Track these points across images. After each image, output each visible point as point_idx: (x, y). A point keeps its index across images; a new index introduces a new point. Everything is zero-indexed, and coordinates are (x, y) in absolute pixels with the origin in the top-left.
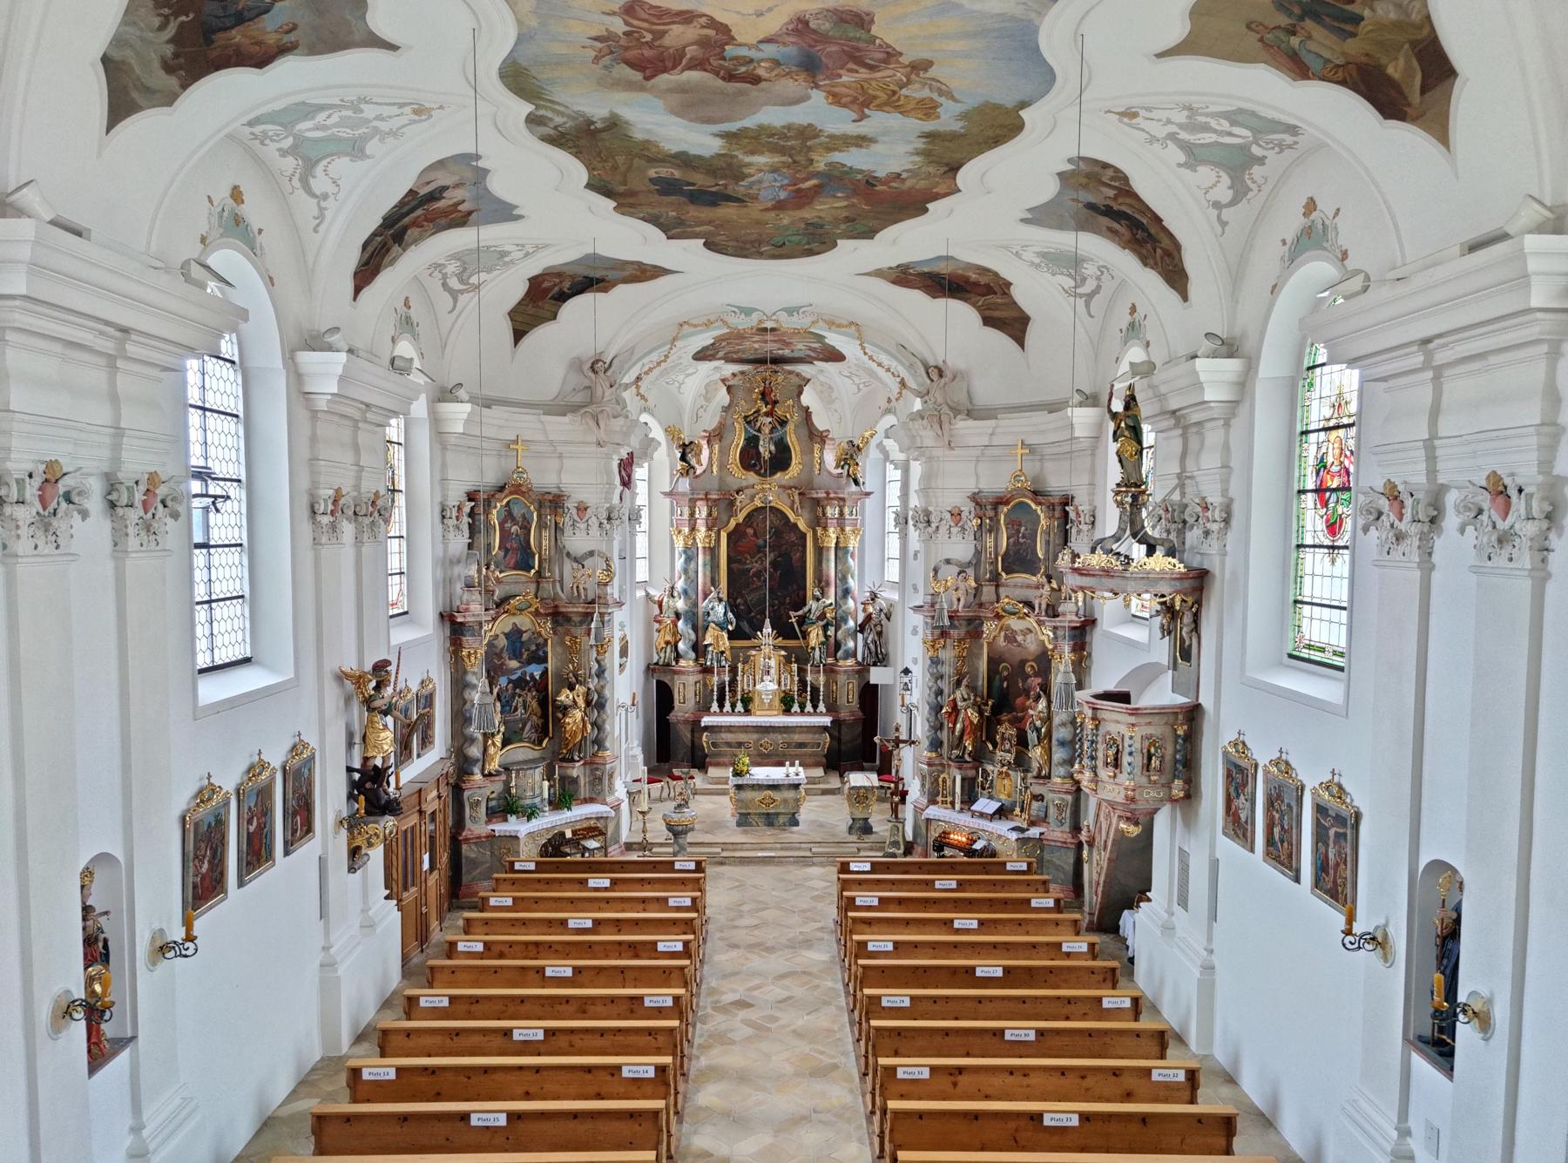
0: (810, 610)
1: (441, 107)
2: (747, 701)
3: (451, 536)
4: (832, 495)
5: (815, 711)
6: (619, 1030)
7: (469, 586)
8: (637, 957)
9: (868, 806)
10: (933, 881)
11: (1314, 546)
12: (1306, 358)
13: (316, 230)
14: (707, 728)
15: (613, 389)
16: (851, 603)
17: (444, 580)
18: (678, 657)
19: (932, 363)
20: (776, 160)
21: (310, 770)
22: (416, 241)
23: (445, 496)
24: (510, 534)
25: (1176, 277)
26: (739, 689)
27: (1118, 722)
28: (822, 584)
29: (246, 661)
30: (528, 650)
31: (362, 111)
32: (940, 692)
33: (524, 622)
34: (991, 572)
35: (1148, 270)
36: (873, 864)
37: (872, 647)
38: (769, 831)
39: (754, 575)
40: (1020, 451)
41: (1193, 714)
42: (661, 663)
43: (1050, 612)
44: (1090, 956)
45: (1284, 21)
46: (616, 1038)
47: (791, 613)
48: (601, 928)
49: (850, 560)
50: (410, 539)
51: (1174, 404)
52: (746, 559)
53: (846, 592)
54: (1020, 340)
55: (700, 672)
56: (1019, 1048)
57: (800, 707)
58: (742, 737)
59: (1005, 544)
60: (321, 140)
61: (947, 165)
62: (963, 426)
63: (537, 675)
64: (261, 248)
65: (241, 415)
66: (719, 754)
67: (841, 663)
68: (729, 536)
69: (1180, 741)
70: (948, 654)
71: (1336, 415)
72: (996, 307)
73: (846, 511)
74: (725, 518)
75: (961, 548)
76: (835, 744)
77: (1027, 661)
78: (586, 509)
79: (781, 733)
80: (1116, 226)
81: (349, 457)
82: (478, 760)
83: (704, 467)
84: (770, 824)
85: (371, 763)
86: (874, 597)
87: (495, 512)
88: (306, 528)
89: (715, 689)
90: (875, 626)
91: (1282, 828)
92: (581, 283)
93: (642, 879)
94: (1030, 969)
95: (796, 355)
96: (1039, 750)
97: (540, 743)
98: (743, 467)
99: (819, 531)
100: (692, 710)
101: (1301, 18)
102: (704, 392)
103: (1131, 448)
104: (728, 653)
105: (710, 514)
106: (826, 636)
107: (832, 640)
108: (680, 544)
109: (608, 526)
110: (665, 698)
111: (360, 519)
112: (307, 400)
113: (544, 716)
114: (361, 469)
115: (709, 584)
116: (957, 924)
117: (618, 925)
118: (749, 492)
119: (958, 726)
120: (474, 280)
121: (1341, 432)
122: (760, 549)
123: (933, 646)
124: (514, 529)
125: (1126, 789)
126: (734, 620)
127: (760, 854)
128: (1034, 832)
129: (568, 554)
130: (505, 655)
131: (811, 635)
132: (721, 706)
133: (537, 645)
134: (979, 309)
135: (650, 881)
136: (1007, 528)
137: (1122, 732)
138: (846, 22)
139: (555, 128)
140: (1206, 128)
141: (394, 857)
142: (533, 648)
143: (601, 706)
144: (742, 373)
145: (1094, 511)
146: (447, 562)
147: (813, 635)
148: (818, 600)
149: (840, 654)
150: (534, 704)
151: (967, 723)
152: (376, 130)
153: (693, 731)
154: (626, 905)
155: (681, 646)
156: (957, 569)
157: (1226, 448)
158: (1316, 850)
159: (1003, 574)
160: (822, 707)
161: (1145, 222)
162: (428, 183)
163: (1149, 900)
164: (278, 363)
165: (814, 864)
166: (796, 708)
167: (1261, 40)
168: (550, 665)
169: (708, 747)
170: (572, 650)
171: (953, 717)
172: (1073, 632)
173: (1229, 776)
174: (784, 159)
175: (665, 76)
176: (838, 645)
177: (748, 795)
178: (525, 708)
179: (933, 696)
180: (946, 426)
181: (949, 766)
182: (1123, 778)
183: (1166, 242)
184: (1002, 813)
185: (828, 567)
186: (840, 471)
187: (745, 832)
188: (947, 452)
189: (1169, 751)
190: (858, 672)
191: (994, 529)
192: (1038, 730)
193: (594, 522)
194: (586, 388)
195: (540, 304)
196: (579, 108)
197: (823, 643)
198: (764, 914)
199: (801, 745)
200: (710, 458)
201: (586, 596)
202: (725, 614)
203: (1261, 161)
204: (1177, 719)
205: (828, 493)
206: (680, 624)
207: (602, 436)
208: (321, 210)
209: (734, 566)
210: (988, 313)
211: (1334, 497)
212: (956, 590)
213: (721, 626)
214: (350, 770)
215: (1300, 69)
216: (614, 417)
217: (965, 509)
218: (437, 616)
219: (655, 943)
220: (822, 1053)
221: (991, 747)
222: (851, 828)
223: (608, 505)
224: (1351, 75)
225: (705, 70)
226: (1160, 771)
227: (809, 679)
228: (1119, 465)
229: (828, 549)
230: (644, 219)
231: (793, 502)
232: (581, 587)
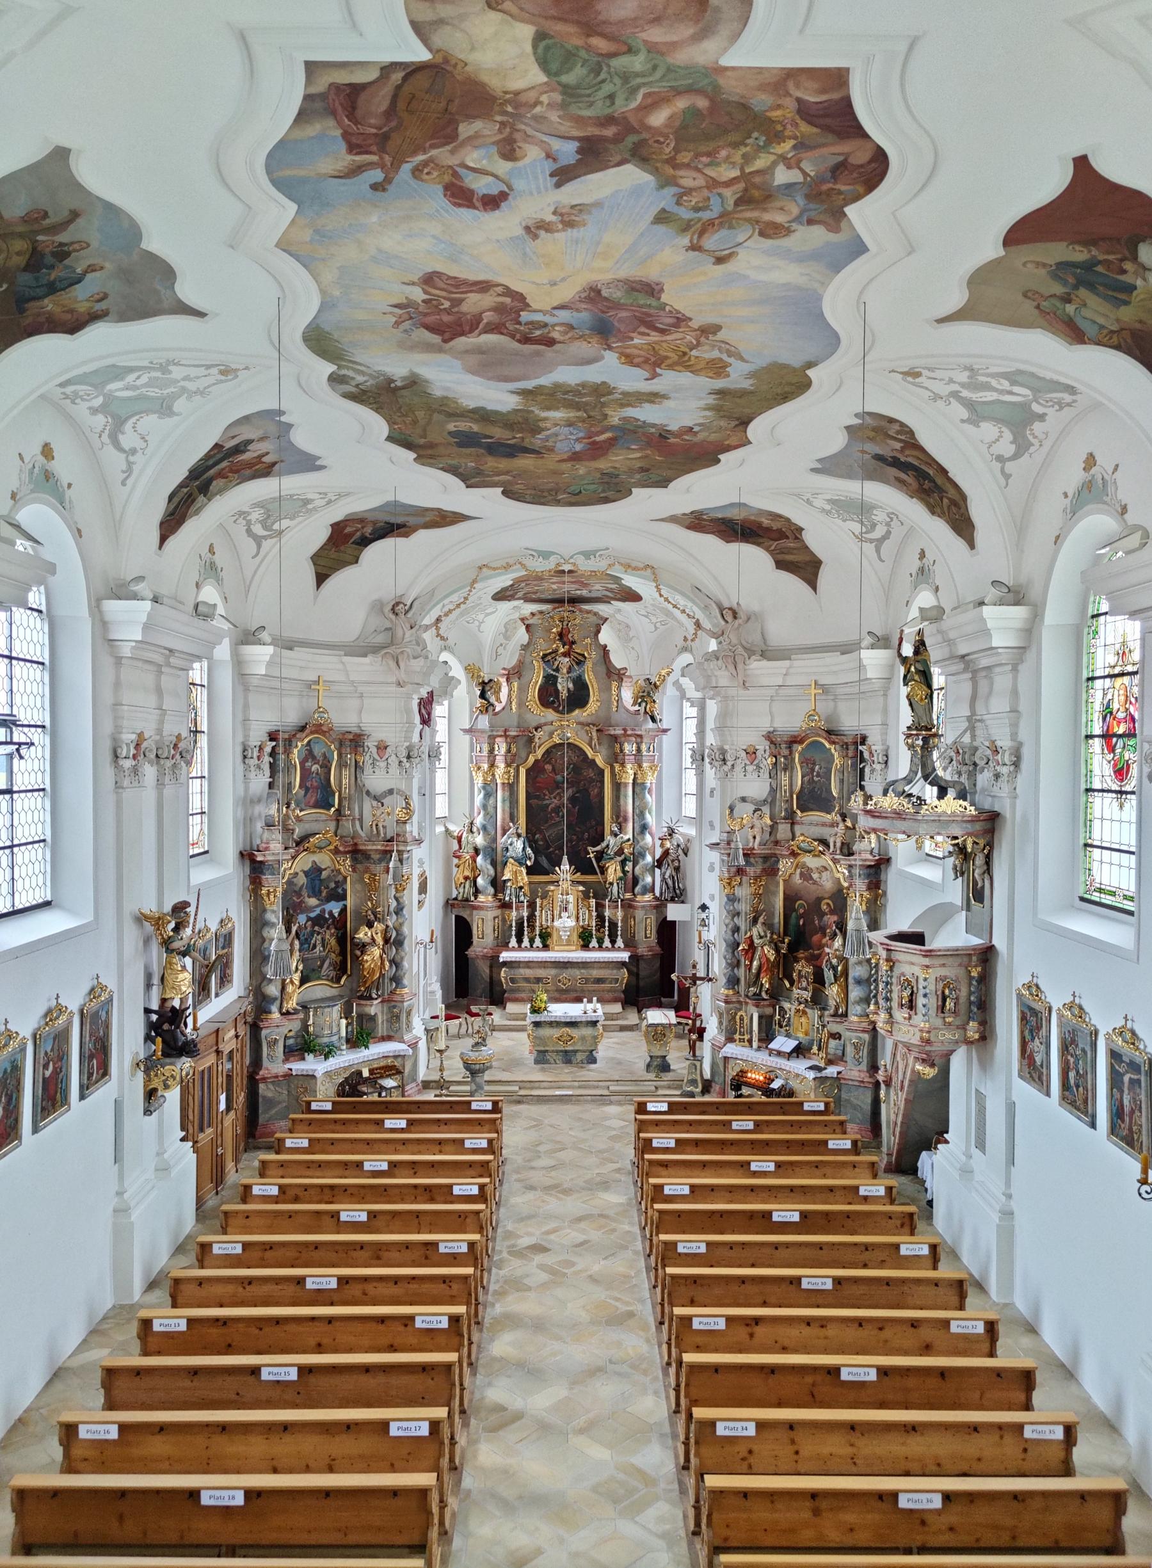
0: (608, 846)
1: (247, 368)
2: (545, 936)
3: (252, 775)
4: (629, 732)
6: (414, 1278)
7: (269, 825)
8: (432, 1200)
9: (666, 1044)
10: (730, 1122)
11: (1103, 791)
12: (1091, 606)
13: (124, 483)
14: (505, 964)
15: (414, 630)
16: (648, 838)
17: (245, 819)
18: (477, 892)
19: (726, 604)
20: (572, 415)
21: (107, 1013)
22: (220, 492)
23: (246, 736)
24: (311, 773)
25: (963, 526)
26: (538, 924)
27: (913, 964)
28: (620, 819)
29: (47, 904)
30: (327, 887)
31: (170, 372)
32: (736, 929)
33: (324, 860)
34: (786, 810)
35: (936, 518)
36: (670, 1104)
37: (670, 882)
38: (567, 1069)
39: (553, 810)
40: (813, 692)
41: (987, 955)
42: (460, 898)
43: (845, 851)
44: (887, 1200)
45: (1059, 289)
46: (411, 1286)
48: (396, 1171)
49: (648, 796)
50: (211, 779)
51: (962, 650)
53: (644, 828)
54: (812, 582)
55: (499, 907)
56: (816, 1298)
58: (541, 973)
59: (800, 782)
60: (129, 399)
61: (738, 419)
62: (757, 666)
63: (336, 912)
64: (70, 502)
65: (47, 662)
66: (518, 990)
67: (639, 898)
68: (528, 772)
69: (974, 983)
70: (744, 892)
71: (1120, 663)
72: (789, 551)
73: (644, 747)
74: (523, 754)
75: (756, 786)
76: (634, 979)
77: (822, 898)
78: (386, 748)
79: (579, 968)
80: (903, 476)
81: (152, 701)
82: (275, 999)
83: (504, 703)
84: (568, 1061)
85: (168, 1005)
86: (671, 832)
87: (295, 751)
88: (109, 772)
90: (673, 861)
91: (1078, 1072)
92: (382, 528)
93: (439, 1120)
94: (827, 1214)
95: (593, 595)
96: (835, 988)
97: (338, 981)
98: (543, 705)
99: (617, 767)
100: (490, 945)
101: (1076, 287)
102: (504, 630)
103: (921, 692)
104: (526, 888)
105: (509, 751)
106: (624, 872)
107: (630, 875)
108: (479, 781)
109: (408, 765)
110: (463, 932)
111: (162, 762)
112: (112, 646)
113: (343, 953)
114: (163, 712)
115: (508, 819)
116: (754, 1167)
117: (414, 1168)
118: (545, 728)
119: (755, 963)
120: (276, 526)
121: (1126, 680)
122: (558, 785)
123: (729, 884)
124: (315, 768)
125: (921, 1031)
126: (533, 856)
127: (557, 1093)
128: (832, 1071)
129: (368, 793)
130: (305, 893)
131: (609, 870)
132: (520, 941)
133: (337, 883)
134: (772, 553)
135: (446, 1122)
136: (802, 767)
137: (916, 974)
138: (637, 291)
139: (357, 386)
140: (987, 387)
141: (191, 1098)
142: (332, 885)
143: (399, 943)
144: (541, 612)
145: (887, 750)
146: (248, 802)
147: (611, 871)
148: (616, 835)
149: (637, 889)
150: (333, 941)
151: (763, 960)
152: (184, 390)
153: (491, 967)
154: (422, 1147)
155: (480, 881)
156: (753, 807)
157: (1015, 693)
158: (1111, 1096)
159: (798, 812)
160: (620, 943)
161: (931, 473)
162: (233, 437)
163: (947, 1142)
164: (84, 612)
165: (611, 1103)
166: (594, 943)
167: (1038, 307)
168: (349, 902)
169: (507, 983)
170: (372, 887)
171: (750, 955)
172: (868, 871)
173: (1023, 1019)
174: (579, 414)
175: (463, 339)
176: (635, 881)
177: (546, 1032)
178: (323, 946)
179: (730, 933)
180: (740, 666)
181: (747, 1003)
182: (918, 1020)
183: (952, 492)
184: (799, 1051)
185: (626, 803)
186: (637, 708)
187: (543, 1070)
188: (742, 692)
189: (964, 992)
190: (656, 907)
191: (788, 767)
192: (834, 968)
193: (393, 760)
194: (387, 629)
195: (342, 548)
196: (380, 368)
197: (620, 879)
198: (562, 1155)
199: (599, 981)
200: (510, 696)
201: (385, 834)
202: (524, 849)
203: (1042, 417)
204: (970, 960)
205: (625, 730)
206: (479, 859)
207: (402, 676)
208: (130, 464)
209: (533, 802)
210: (780, 557)
211: (1120, 743)
212: (752, 828)
213: (520, 862)
214: (148, 1011)
215: (1076, 334)
216: (415, 658)
217: (760, 748)
218: (237, 853)
219: (450, 1187)
220: (617, 1299)
221: (788, 985)
222: (648, 1066)
223: (407, 744)
224: (1125, 341)
225: (502, 334)
226: (955, 1012)
227: (607, 913)
228: (909, 708)
229: (626, 784)
230: (442, 469)
231: (591, 738)
232: (380, 825)
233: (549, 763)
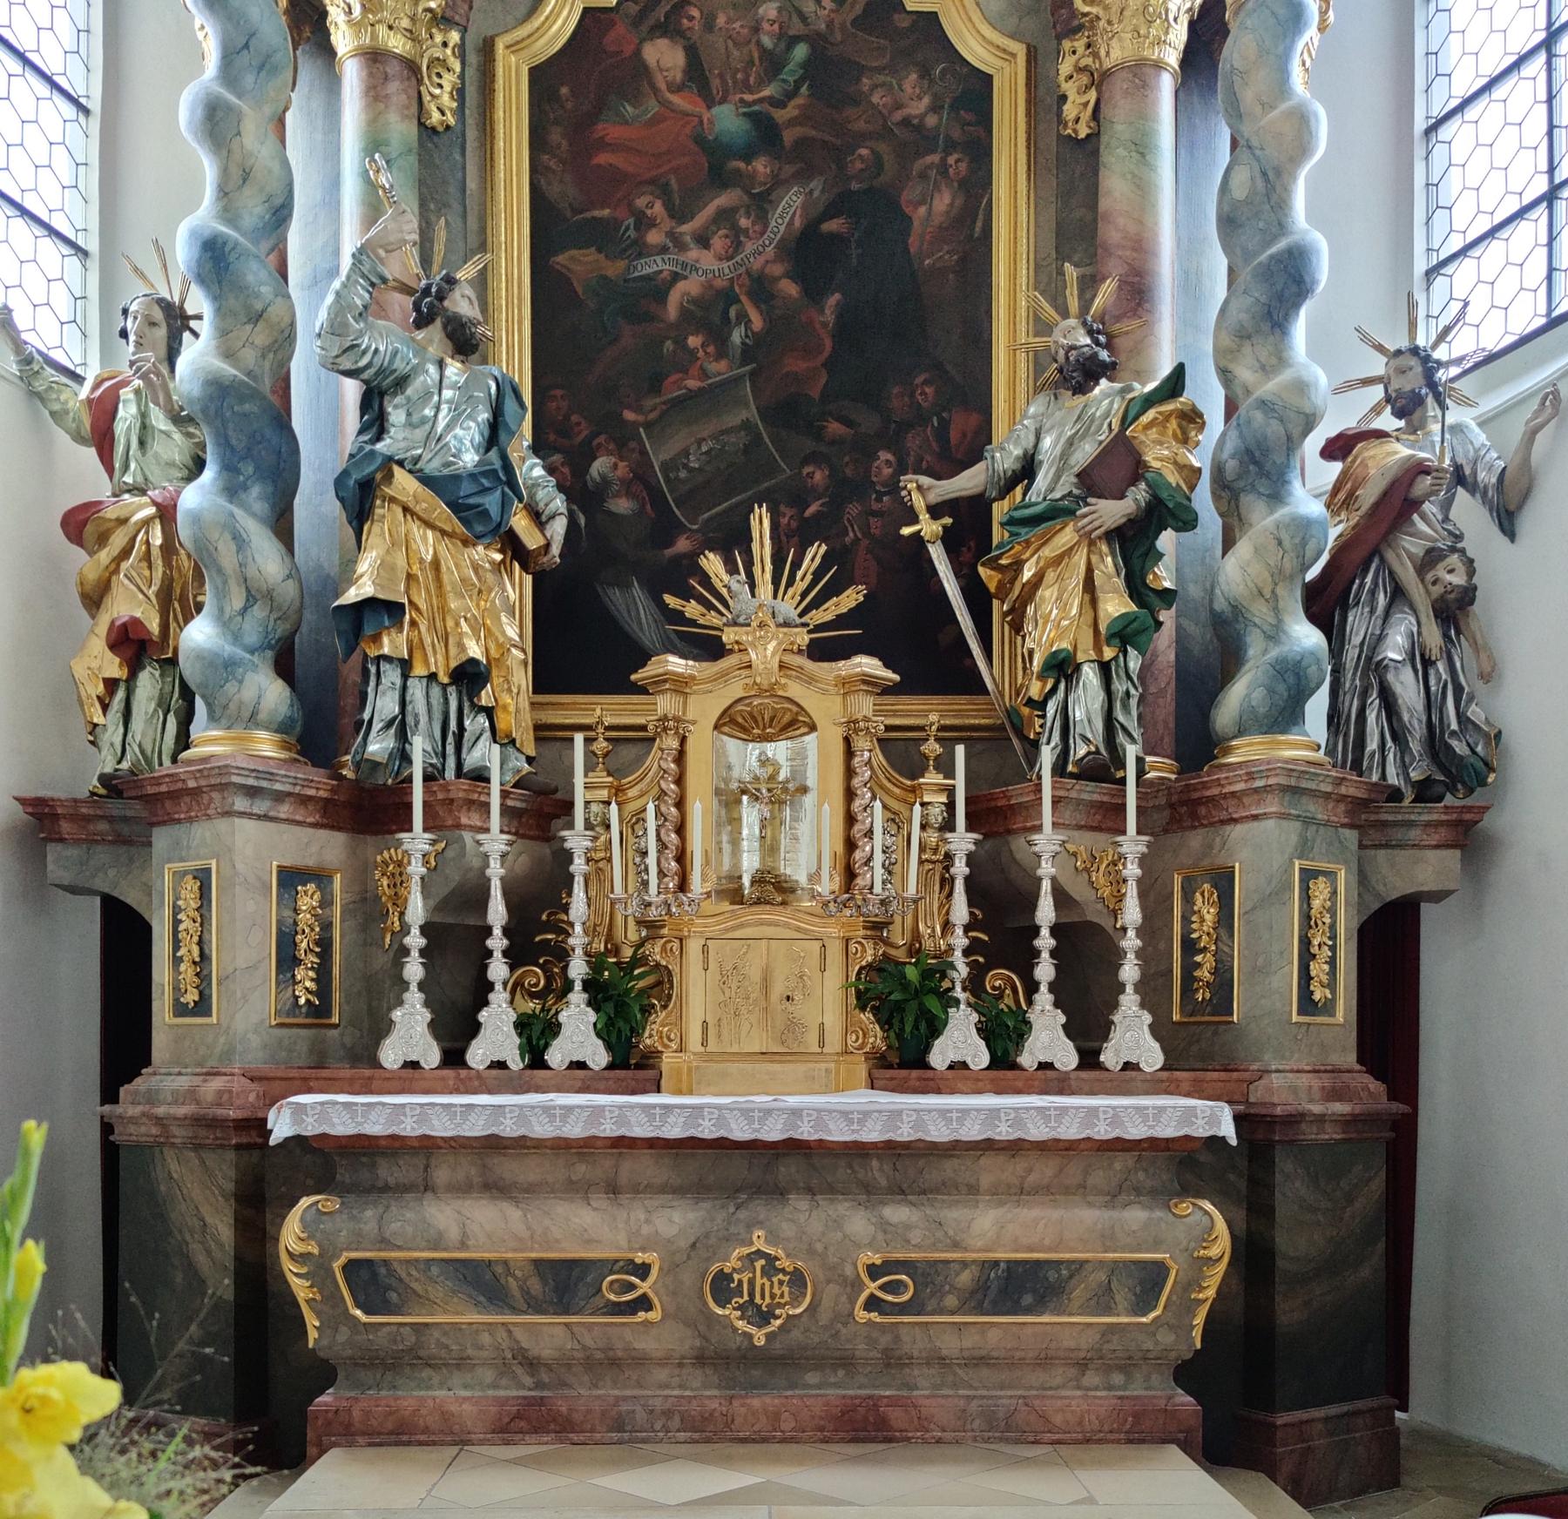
0: (1027, 469)
5: (1089, 1059)
47: (910, 482)
52: (644, 222)
57: (987, 1032)
67: (1246, 751)
79: (869, 1193)
89: (417, 909)
90: (1431, 558)
169: (334, 1316)
185: (1143, 189)
197: (1125, 635)
229: (1142, 71)
233: (668, 28)
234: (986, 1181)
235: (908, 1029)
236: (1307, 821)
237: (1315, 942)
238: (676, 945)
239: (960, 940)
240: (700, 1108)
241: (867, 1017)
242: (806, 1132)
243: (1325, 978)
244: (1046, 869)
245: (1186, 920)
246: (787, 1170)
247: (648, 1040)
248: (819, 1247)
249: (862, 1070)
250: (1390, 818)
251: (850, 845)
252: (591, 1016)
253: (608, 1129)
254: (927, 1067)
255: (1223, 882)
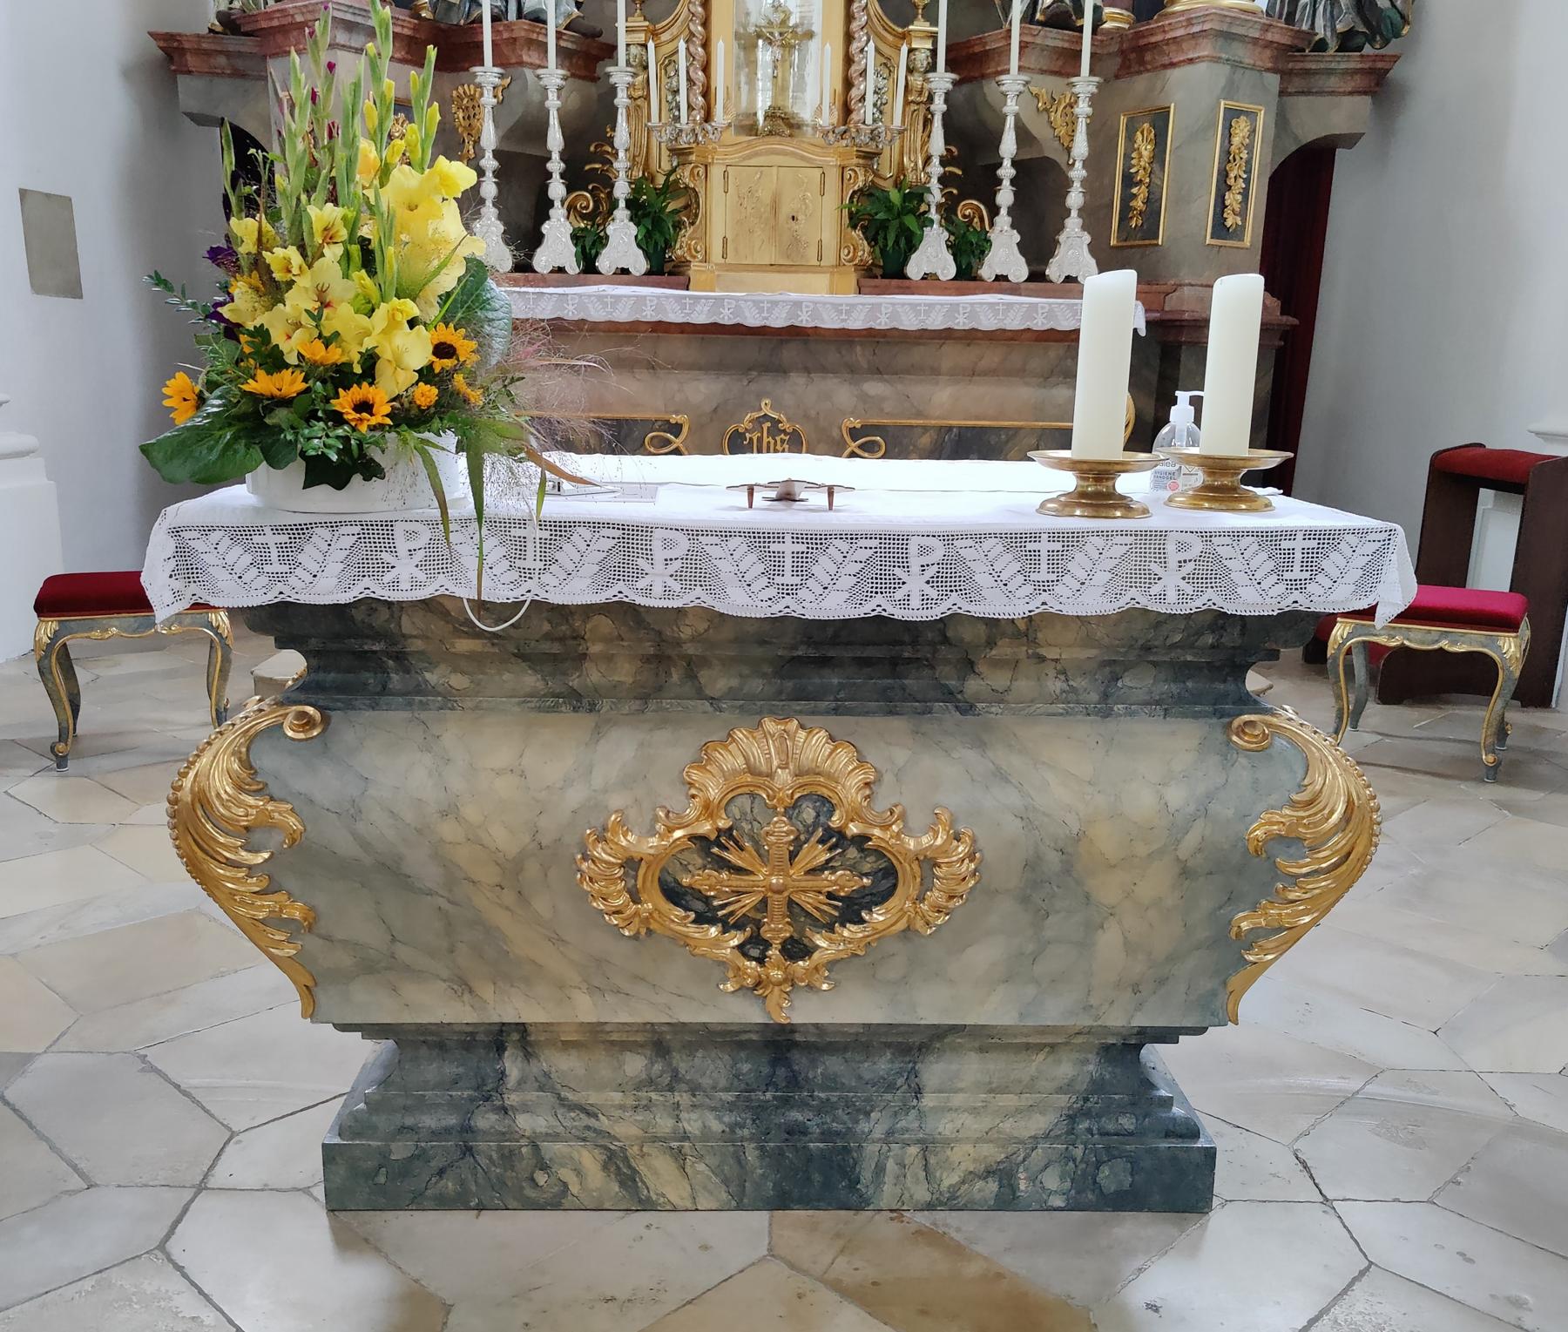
57: (956, 249)
79: (853, 372)
234: (946, 364)
235: (890, 243)
236: (1236, 65)
237: (1232, 175)
238: (702, 170)
239: (936, 169)
240: (722, 299)
241: (857, 234)
242: (804, 320)
243: (1237, 207)
244: (1011, 107)
245: (1127, 157)
246: (790, 353)
247: (679, 252)
248: (813, 413)
249: (852, 278)
250: (1313, 66)
251: (848, 84)
252: (633, 229)
253: (649, 315)
254: (905, 277)
255: (1160, 119)
